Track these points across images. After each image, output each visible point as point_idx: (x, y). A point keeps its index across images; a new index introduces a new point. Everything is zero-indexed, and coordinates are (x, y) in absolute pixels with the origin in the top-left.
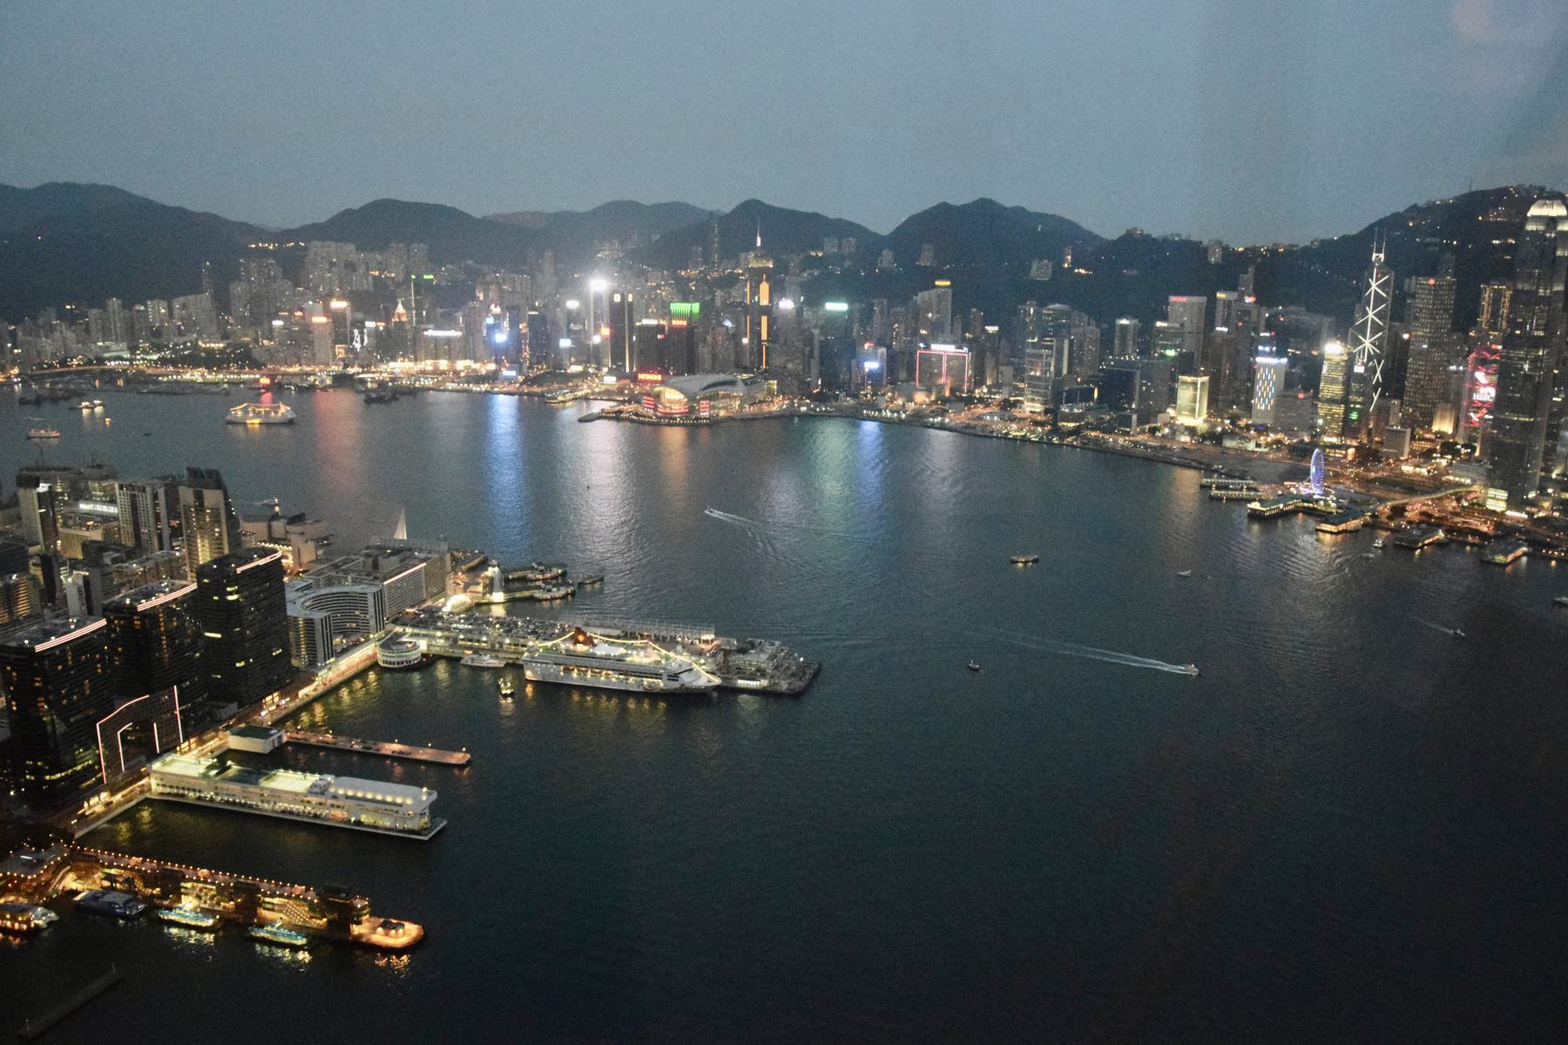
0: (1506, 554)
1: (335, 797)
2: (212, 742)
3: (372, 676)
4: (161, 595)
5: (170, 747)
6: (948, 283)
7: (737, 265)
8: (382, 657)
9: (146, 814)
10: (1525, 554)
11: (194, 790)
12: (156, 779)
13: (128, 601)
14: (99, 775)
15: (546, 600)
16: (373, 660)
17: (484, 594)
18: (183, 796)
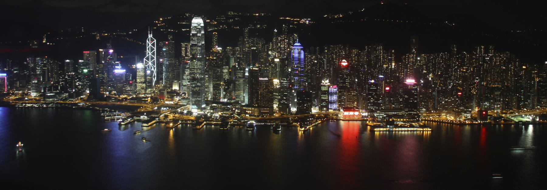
0: (200, 125)
10: (205, 124)
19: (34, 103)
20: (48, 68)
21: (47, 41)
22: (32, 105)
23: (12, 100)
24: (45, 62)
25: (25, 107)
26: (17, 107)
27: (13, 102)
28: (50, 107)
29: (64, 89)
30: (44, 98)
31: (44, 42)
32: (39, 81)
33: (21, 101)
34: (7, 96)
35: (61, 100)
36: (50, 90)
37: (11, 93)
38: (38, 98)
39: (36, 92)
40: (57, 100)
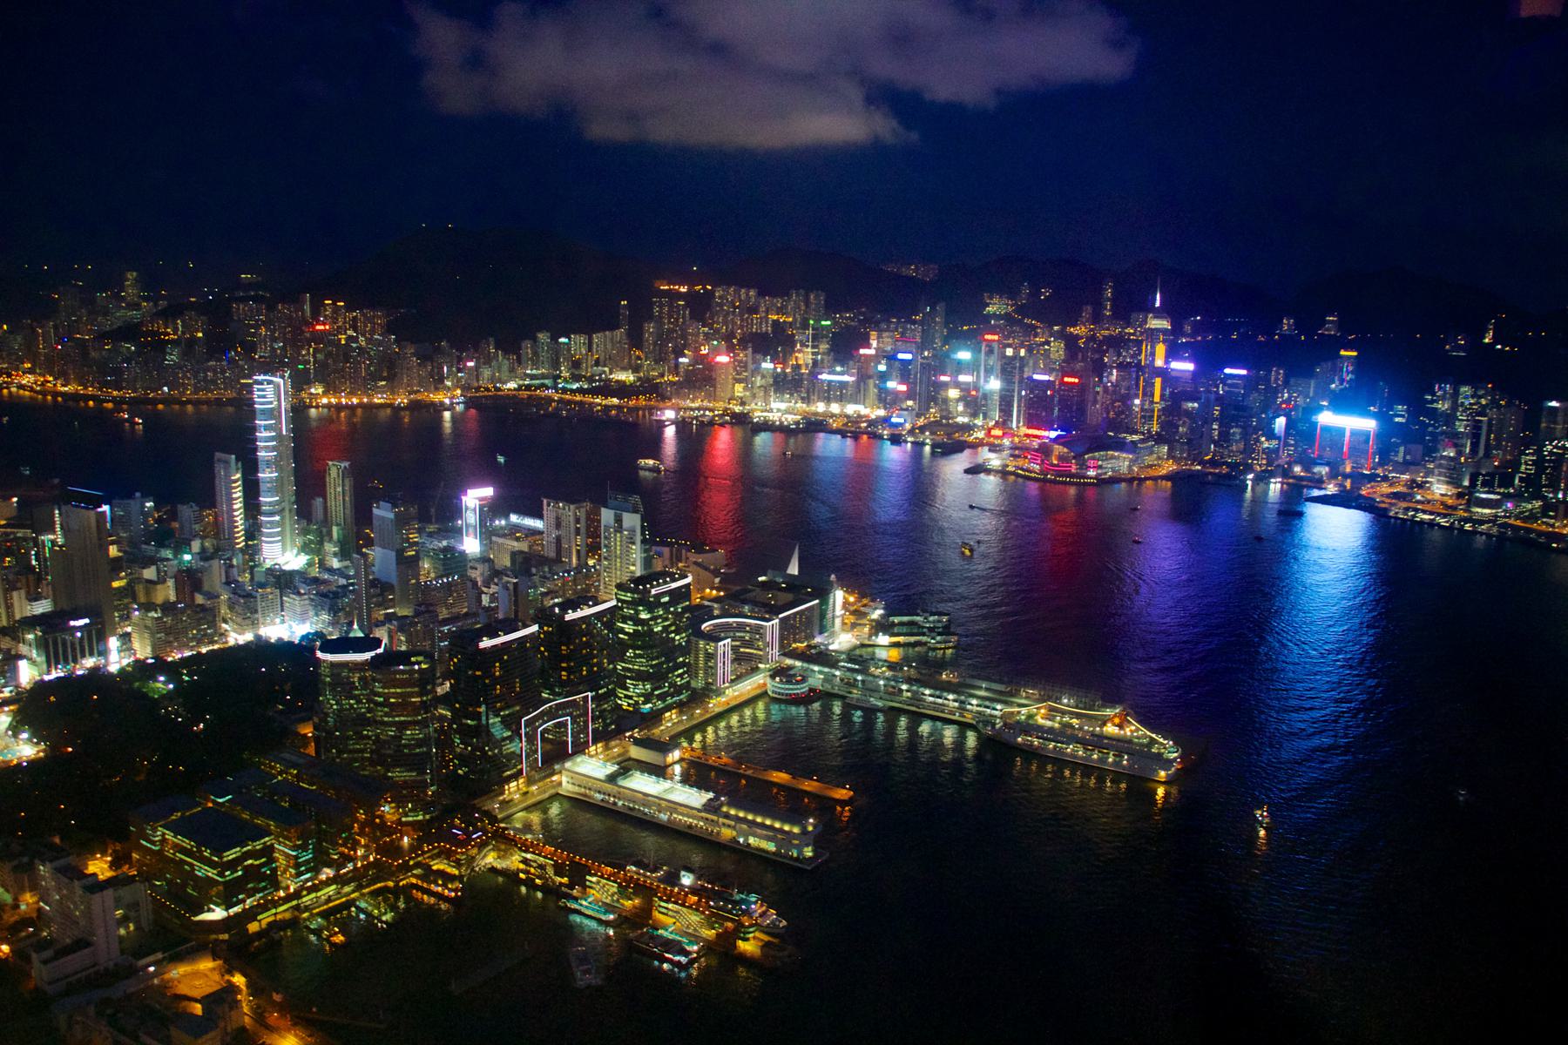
1: (727, 816)
2: (616, 750)
3: (761, 705)
4: (585, 607)
5: (580, 749)
6: (1355, 354)
7: (1128, 325)
8: (774, 686)
9: (555, 810)
11: (599, 792)
12: (567, 776)
13: (557, 610)
14: (519, 767)
15: (941, 649)
16: (763, 689)
17: (870, 636)
18: (589, 797)
19: (1439, 514)
20: (1490, 420)
21: (1496, 340)
22: (1432, 517)
23: (1382, 495)
24: (1483, 402)
25: (1412, 520)
26: (1391, 517)
27: (1383, 502)
28: (1481, 534)
29: (1532, 486)
30: (1469, 504)
31: (1487, 341)
32: (1460, 454)
33: (1404, 500)
34: (1369, 482)
35: (1517, 518)
36: (1489, 485)
37: (1379, 476)
38: (1450, 502)
39: (1448, 483)
40: (1505, 517)
